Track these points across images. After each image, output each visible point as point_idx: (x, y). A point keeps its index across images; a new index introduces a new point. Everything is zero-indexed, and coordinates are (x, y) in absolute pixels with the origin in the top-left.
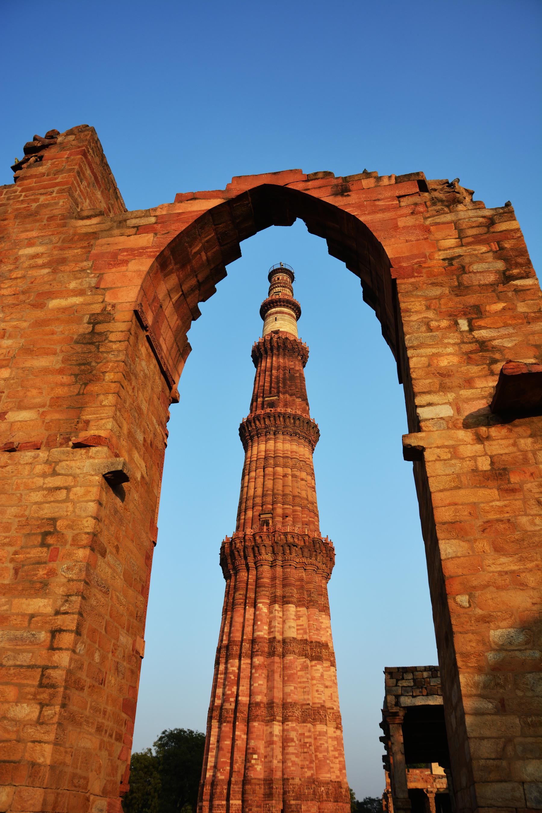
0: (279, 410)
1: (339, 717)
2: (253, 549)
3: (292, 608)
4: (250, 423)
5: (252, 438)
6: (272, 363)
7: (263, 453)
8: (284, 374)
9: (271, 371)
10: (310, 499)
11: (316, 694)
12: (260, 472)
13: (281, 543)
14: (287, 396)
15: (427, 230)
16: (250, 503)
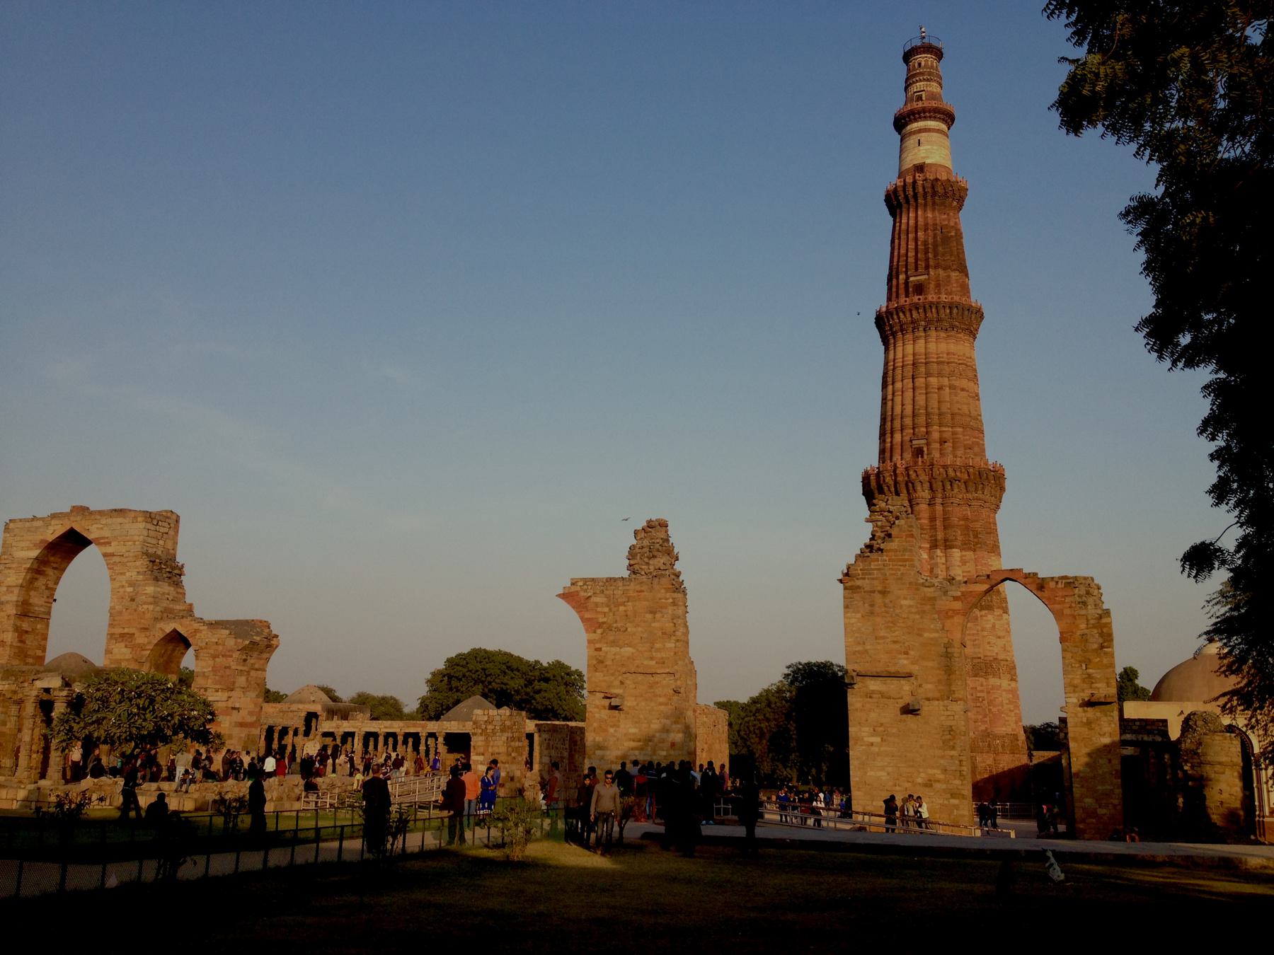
0: (930, 298)
1: (1014, 668)
2: (907, 485)
3: (956, 553)
4: (892, 314)
5: (894, 334)
6: (916, 217)
7: (911, 358)
8: (935, 236)
9: (916, 232)
10: (974, 413)
11: (988, 647)
12: (908, 382)
13: (940, 478)
14: (941, 271)
15: (1074, 617)
16: (897, 424)
